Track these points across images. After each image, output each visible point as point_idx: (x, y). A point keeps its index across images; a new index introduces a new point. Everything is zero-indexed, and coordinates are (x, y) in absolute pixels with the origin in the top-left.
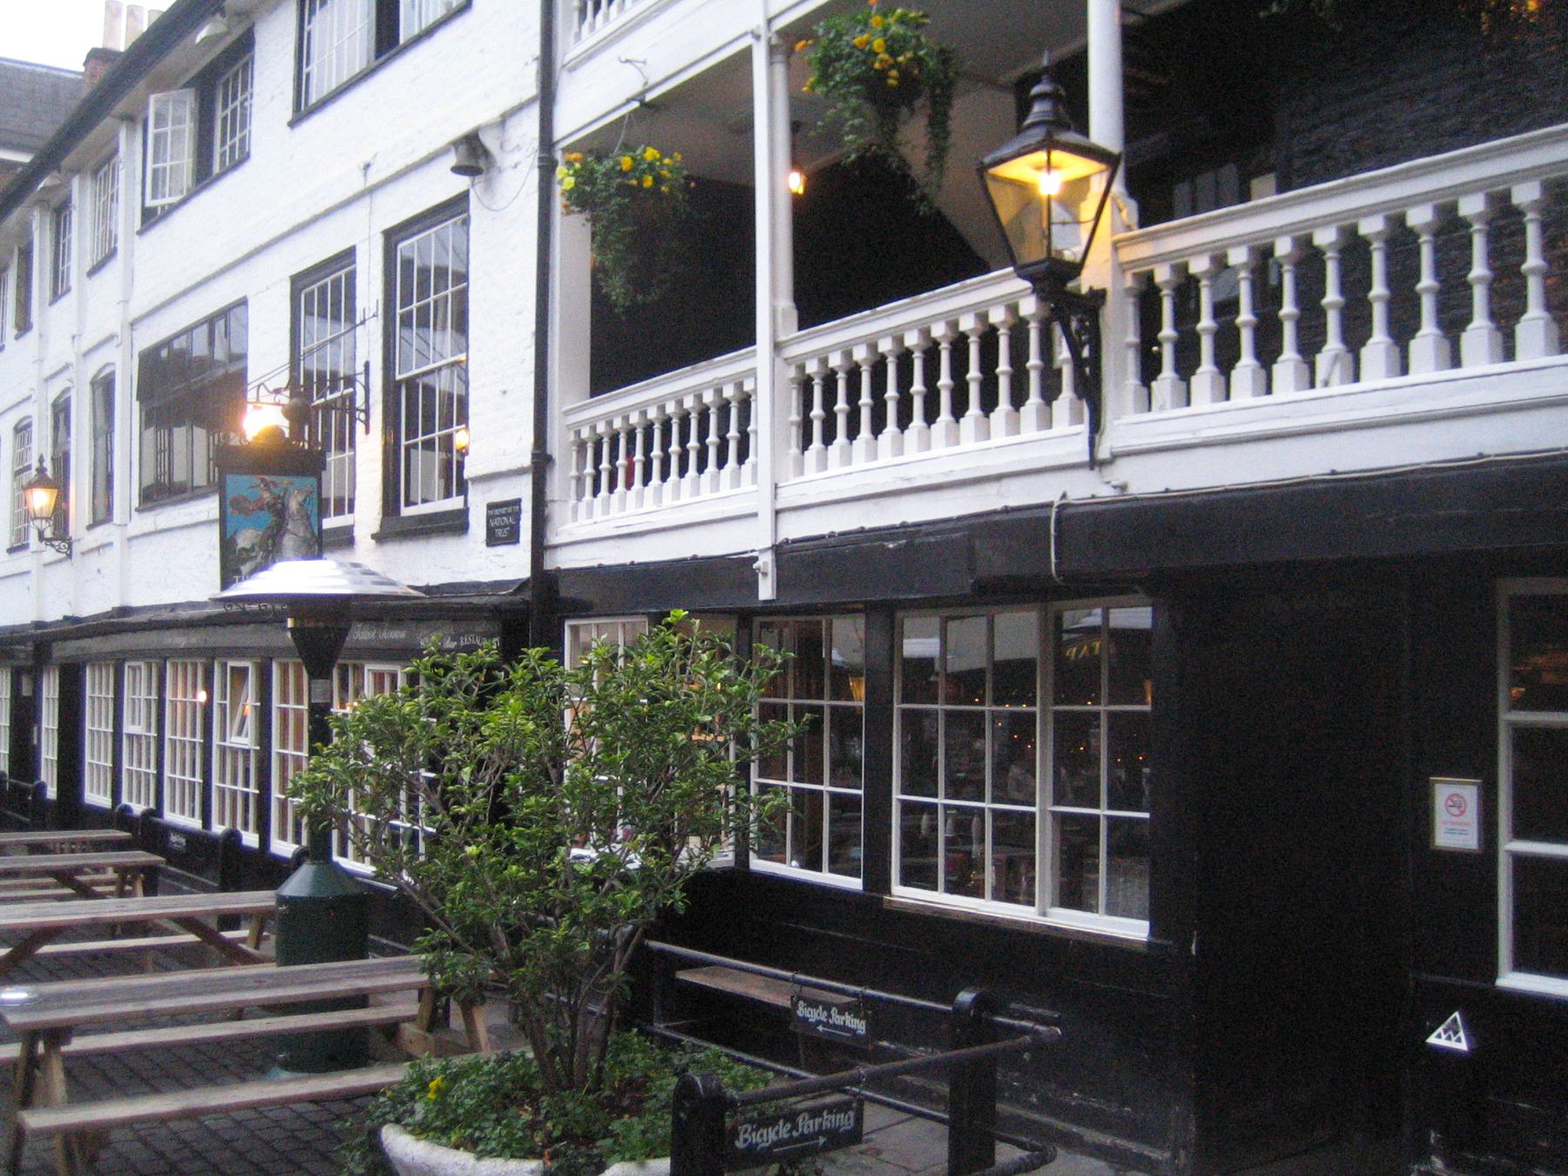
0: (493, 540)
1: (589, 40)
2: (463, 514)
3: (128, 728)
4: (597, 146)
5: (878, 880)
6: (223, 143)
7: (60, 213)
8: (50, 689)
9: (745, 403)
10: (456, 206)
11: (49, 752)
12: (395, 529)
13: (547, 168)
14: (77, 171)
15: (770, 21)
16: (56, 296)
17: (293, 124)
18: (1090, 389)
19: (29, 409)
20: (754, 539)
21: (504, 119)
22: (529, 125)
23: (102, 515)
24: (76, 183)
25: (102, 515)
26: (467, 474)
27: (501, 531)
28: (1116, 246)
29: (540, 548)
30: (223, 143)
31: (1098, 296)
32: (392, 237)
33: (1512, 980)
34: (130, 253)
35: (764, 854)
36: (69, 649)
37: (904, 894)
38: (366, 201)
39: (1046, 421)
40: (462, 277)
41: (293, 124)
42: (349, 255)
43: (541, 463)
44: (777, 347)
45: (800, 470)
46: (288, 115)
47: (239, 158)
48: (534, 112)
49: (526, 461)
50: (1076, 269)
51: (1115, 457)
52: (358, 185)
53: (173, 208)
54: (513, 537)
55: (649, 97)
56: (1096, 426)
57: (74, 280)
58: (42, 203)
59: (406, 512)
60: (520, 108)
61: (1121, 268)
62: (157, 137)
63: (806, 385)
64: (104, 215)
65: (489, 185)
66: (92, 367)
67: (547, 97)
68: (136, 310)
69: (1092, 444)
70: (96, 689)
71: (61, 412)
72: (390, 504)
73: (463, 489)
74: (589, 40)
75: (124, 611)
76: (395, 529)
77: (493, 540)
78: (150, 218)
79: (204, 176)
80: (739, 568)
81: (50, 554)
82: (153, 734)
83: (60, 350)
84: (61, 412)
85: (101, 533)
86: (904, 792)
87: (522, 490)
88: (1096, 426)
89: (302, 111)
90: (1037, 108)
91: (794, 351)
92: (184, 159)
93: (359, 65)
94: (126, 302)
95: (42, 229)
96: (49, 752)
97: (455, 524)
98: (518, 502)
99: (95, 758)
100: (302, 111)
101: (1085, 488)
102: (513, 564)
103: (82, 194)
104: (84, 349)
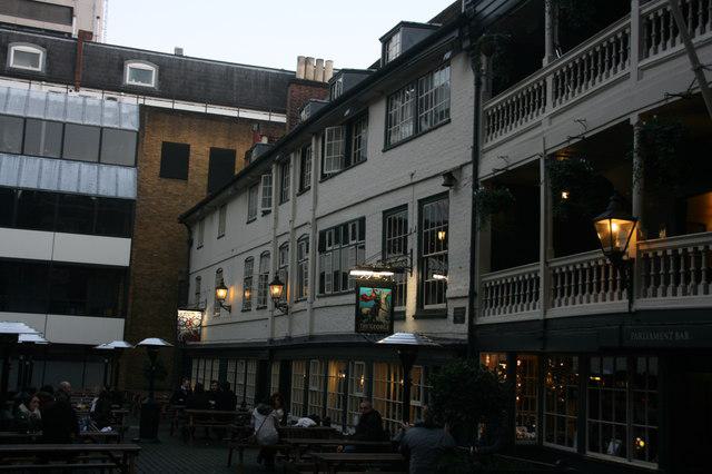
0: (456, 321)
1: (490, 144)
2: (446, 310)
3: (312, 388)
6: (355, 149)
8: (275, 371)
9: (538, 279)
10: (444, 195)
15: (545, 151)
16: (281, 203)
17: (384, 151)
19: (269, 248)
21: (462, 166)
22: (469, 171)
24: (292, 155)
25: (300, 296)
26: (448, 296)
27: (458, 319)
28: (638, 245)
30: (355, 149)
31: (632, 260)
32: (421, 202)
34: (316, 188)
35: (547, 440)
37: (590, 454)
38: (411, 188)
39: (620, 298)
40: (447, 222)
41: (384, 151)
42: (406, 205)
43: (472, 294)
44: (546, 263)
45: (553, 306)
46: (381, 145)
47: (361, 160)
48: (471, 166)
49: (467, 294)
50: (624, 253)
51: (638, 312)
52: (409, 181)
53: (336, 174)
54: (463, 322)
55: (510, 168)
56: (631, 302)
57: (291, 196)
58: (278, 162)
59: (426, 307)
60: (466, 164)
61: (639, 252)
62: (329, 146)
63: (555, 276)
65: (456, 190)
66: (299, 233)
67: (476, 162)
68: (318, 215)
69: (630, 307)
70: (298, 371)
73: (446, 302)
74: (490, 144)
75: (312, 337)
77: (456, 321)
78: (325, 177)
81: (277, 312)
82: (322, 390)
83: (284, 226)
85: (300, 306)
86: (590, 417)
87: (465, 304)
88: (631, 302)
89: (388, 147)
90: (612, 203)
91: (552, 265)
92: (338, 154)
94: (314, 210)
95: (276, 176)
97: (442, 315)
98: (464, 308)
100: (388, 147)
103: (295, 162)
104: (296, 226)
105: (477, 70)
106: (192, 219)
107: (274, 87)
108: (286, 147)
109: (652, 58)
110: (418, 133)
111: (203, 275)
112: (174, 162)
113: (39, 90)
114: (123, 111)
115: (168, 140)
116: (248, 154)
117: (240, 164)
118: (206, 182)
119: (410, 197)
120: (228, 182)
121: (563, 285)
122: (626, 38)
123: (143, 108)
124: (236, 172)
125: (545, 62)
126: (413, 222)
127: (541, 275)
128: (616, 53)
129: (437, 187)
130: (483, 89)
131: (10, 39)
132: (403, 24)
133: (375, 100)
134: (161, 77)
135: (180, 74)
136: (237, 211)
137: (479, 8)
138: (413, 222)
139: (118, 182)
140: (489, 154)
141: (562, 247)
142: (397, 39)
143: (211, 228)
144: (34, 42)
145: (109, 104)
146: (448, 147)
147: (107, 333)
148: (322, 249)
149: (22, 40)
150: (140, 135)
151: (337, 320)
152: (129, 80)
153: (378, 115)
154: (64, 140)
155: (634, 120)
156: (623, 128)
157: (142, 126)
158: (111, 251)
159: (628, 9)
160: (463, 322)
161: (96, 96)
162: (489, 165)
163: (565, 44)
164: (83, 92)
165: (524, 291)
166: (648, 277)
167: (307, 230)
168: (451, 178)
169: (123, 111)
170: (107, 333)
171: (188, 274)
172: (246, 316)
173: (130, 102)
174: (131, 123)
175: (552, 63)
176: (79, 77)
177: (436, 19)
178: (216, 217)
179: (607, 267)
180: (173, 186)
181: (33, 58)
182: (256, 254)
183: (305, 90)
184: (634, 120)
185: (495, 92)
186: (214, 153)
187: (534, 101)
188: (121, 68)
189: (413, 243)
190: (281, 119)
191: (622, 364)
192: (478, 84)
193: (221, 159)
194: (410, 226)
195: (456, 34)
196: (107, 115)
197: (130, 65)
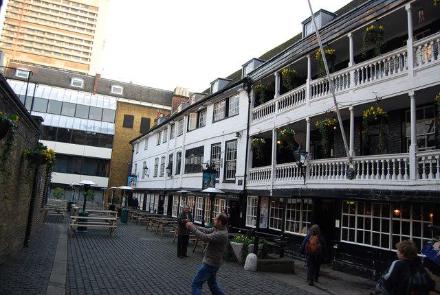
4: (254, 137)
5: (283, 230)
7: (173, 125)
8: (166, 199)
11: (166, 209)
12: (225, 181)
13: (248, 138)
14: (176, 120)
18: (305, 177)
20: (270, 188)
23: (178, 172)
25: (178, 172)
27: (240, 183)
29: (245, 186)
32: (226, 142)
33: (342, 241)
36: (170, 194)
37: (286, 232)
42: (220, 143)
43: (245, 176)
54: (241, 185)
64: (181, 127)
71: (171, 156)
72: (225, 178)
76: (225, 181)
78: (188, 131)
79: (197, 127)
80: (269, 191)
84: (171, 156)
87: (243, 179)
89: (214, 122)
93: (223, 117)
96: (166, 209)
97: (234, 182)
99: (174, 210)
100: (214, 122)
101: (304, 187)
102: (241, 188)
103: (177, 123)
105: (249, 97)
106: (132, 142)
107: (169, 97)
108: (171, 119)
109: (314, 99)
110: (227, 116)
111: (139, 163)
112: (128, 122)
113: (82, 94)
114: (110, 103)
115: (126, 114)
116: (156, 120)
117: (152, 125)
118: (139, 129)
119: (223, 140)
120: (146, 129)
121: (280, 174)
122: (304, 92)
123: (118, 102)
124: (151, 127)
125: (275, 96)
126: (223, 149)
127: (272, 170)
128: (302, 96)
129: (234, 137)
130: (251, 103)
131: (72, 76)
132: (219, 79)
133: (211, 104)
134: (124, 91)
135: (132, 91)
136: (153, 139)
137: (251, 77)
138: (223, 149)
139: (108, 127)
140: (253, 127)
141: (279, 162)
142: (217, 84)
143: (142, 145)
144: (80, 77)
145: (105, 100)
146: (237, 123)
147: (102, 182)
148: (187, 156)
149: (76, 76)
150: (116, 112)
151: (194, 181)
152: (112, 92)
153: (210, 109)
154: (88, 112)
155: (307, 119)
156: (304, 121)
157: (117, 109)
158: (104, 153)
159: (306, 82)
160: (241, 185)
161: (101, 97)
162: (254, 131)
163: (282, 91)
164: (96, 95)
165: (266, 175)
166: (311, 173)
167: (181, 150)
168: (238, 134)
169: (110, 103)
170: (102, 182)
171: (132, 162)
172: (155, 179)
173: (113, 100)
174: (114, 107)
175: (277, 98)
176: (95, 90)
177: (230, 77)
178: (144, 141)
179: (296, 169)
180: (127, 130)
181: (80, 84)
182: (160, 157)
183: (178, 99)
184: (307, 119)
185: (257, 104)
186: (143, 119)
187: (272, 109)
188: (110, 87)
189: (223, 156)
190: (169, 108)
191: (299, 200)
192: (250, 102)
193: (145, 122)
194: (222, 150)
195: (243, 84)
196: (105, 104)
197: (113, 87)
